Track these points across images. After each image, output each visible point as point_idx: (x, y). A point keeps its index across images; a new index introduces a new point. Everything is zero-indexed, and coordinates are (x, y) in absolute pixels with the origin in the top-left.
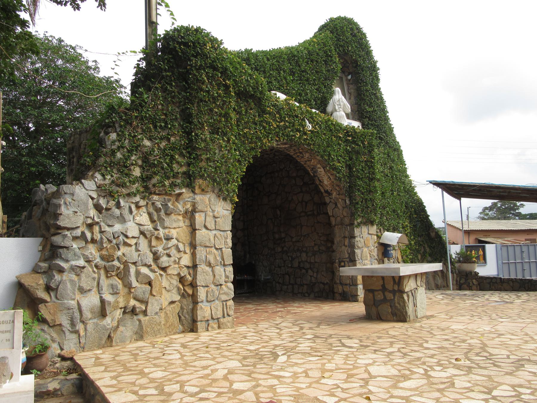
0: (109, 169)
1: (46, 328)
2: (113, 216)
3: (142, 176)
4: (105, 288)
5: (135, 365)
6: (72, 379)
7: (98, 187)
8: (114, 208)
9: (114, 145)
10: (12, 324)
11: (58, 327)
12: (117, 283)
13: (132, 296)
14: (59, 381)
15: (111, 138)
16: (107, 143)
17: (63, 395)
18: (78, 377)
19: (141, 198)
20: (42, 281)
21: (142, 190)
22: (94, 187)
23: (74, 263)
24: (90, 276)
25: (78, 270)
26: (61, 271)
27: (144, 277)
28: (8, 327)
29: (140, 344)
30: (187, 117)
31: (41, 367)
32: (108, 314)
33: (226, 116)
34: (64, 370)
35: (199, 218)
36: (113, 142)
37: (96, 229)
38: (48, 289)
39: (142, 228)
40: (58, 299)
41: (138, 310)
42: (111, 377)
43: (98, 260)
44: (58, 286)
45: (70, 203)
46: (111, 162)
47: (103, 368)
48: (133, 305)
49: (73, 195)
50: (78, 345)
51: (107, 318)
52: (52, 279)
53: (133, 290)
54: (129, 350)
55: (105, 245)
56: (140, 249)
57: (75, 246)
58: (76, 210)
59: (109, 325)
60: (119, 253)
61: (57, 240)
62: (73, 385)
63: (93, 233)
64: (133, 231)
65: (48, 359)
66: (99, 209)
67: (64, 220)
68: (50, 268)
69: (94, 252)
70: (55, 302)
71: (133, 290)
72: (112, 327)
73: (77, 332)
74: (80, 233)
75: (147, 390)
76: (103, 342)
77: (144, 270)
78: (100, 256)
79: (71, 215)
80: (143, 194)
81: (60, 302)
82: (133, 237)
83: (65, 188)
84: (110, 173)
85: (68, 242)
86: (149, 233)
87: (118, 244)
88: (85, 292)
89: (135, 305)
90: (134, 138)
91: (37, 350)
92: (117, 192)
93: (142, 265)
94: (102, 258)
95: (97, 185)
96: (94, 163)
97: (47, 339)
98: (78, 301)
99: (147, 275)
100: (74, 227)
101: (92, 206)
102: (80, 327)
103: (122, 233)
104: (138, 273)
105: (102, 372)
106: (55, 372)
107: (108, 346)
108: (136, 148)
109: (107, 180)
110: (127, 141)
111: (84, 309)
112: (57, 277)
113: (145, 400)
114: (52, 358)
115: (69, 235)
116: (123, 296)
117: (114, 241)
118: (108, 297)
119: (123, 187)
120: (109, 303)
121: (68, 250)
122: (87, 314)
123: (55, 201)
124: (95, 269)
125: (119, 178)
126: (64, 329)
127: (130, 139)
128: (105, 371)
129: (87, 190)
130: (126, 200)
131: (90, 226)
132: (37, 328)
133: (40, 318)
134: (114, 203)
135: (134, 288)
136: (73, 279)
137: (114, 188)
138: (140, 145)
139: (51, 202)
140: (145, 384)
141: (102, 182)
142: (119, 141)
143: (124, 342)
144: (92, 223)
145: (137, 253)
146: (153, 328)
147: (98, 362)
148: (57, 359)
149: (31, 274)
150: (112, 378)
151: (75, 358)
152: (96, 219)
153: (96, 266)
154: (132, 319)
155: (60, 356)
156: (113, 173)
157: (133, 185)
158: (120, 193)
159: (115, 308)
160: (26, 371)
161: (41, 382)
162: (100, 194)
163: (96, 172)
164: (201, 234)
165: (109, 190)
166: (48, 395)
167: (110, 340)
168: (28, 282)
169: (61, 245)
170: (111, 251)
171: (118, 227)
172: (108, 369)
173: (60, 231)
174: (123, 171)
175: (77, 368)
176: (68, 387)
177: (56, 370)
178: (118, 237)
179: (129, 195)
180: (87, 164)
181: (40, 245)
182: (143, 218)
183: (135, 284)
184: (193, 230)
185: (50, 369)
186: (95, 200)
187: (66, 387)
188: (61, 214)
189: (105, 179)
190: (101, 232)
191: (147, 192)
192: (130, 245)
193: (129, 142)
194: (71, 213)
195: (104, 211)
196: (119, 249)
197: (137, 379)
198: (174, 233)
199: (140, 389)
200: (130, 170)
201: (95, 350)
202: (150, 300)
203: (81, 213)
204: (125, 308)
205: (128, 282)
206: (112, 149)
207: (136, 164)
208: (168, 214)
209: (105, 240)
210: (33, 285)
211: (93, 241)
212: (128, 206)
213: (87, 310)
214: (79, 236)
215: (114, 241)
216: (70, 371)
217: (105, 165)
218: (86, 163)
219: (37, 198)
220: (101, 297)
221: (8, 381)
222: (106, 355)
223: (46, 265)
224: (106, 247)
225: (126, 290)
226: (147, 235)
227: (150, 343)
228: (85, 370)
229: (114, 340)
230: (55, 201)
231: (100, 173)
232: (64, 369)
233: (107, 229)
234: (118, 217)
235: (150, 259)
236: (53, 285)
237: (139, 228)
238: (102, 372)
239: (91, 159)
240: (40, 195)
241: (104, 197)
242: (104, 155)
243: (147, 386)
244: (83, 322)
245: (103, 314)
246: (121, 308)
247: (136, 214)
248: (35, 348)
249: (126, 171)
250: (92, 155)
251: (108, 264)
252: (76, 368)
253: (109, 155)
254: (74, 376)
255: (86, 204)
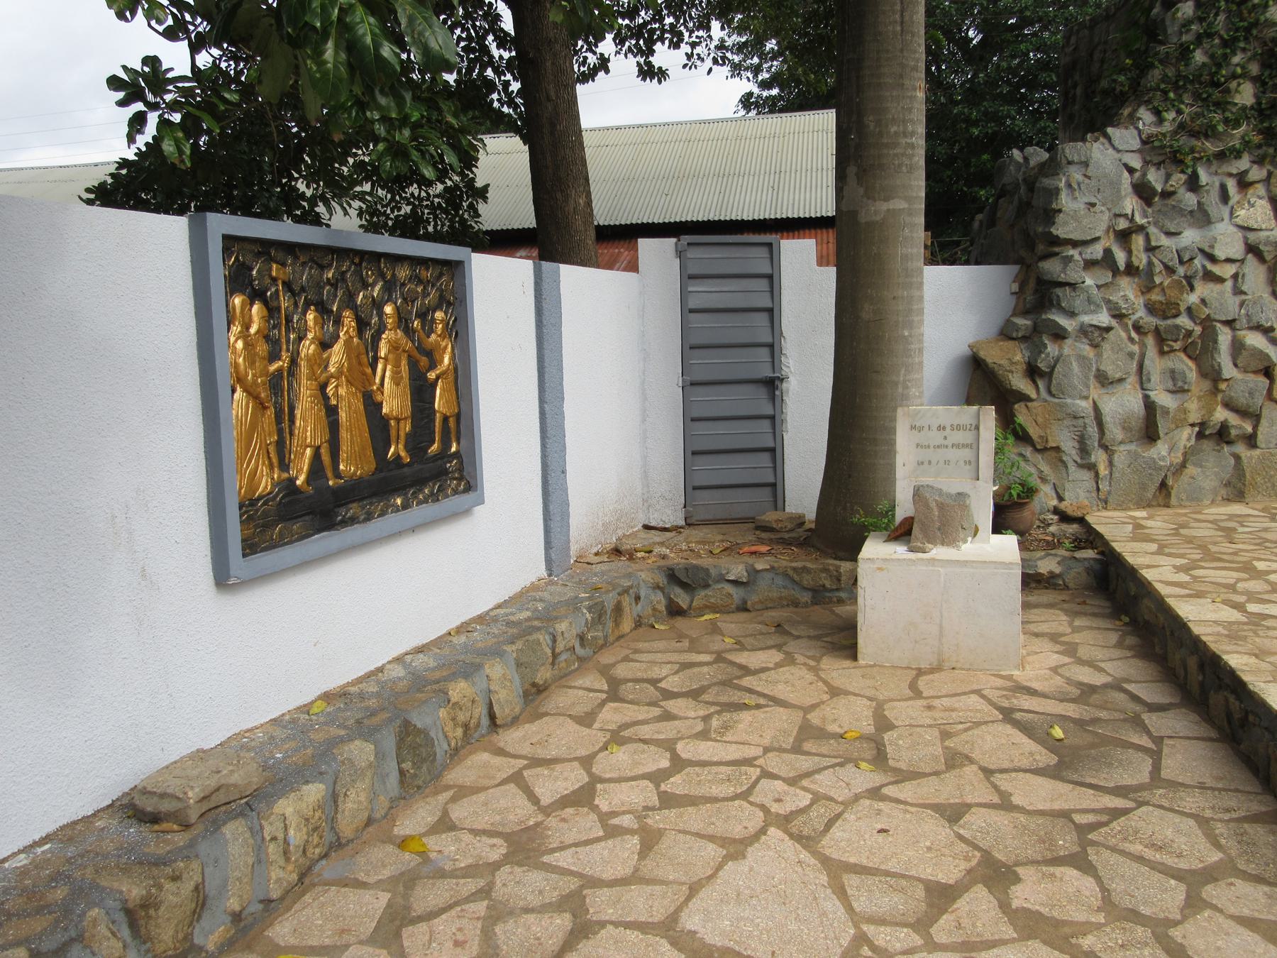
0: (1172, 95)
1: (1028, 451)
2: (1180, 211)
3: (1259, 103)
4: (1155, 378)
5: (1231, 551)
6: (1085, 559)
7: (1144, 142)
8: (1182, 191)
9: (1188, 31)
10: (974, 432)
11: (1053, 454)
12: (1185, 368)
13: (1219, 398)
14: (1059, 559)
15: (1179, 15)
16: (1170, 31)
17: (1067, 587)
18: (1098, 557)
19: (1254, 162)
20: (1019, 355)
21: (1257, 139)
22: (1136, 144)
23: (1086, 319)
24: (1121, 350)
25: (1095, 335)
26: (1059, 335)
27: (1252, 355)
28: (967, 437)
29: (1237, 509)
31: (1022, 527)
32: (1161, 435)
34: (1066, 541)
36: (1184, 26)
37: (1138, 241)
38: (1033, 372)
39: (1252, 237)
40: (1054, 396)
41: (1233, 432)
42: (1175, 567)
43: (1141, 313)
44: (1053, 368)
45: (1079, 184)
46: (1179, 76)
47: (1154, 547)
48: (1222, 419)
49: (1086, 164)
50: (1094, 495)
51: (1159, 443)
52: (1041, 352)
53: (1223, 386)
54: (1211, 518)
55: (1157, 280)
56: (1244, 288)
57: (1089, 282)
58: (1093, 200)
59: (1163, 458)
60: (1193, 298)
61: (1051, 267)
62: (1088, 571)
63: (1130, 252)
64: (1228, 242)
65: (1034, 514)
66: (1145, 195)
67: (1066, 223)
68: (1037, 330)
69: (1131, 296)
70: (1046, 401)
71: (1223, 386)
72: (1171, 465)
73: (1092, 467)
74: (1101, 252)
75: (1267, 606)
76: (1149, 495)
77: (1255, 340)
78: (1145, 306)
79: (1082, 213)
80: (1261, 152)
81: (1056, 400)
82: (1229, 260)
83: (1071, 150)
84: (1174, 106)
85: (1073, 274)
86: (1270, 248)
87: (1191, 277)
88: (1112, 383)
89: (1226, 420)
90: (1243, 7)
91: (1014, 493)
92: (1192, 150)
93: (1251, 328)
94: (1151, 309)
95: (1143, 136)
96: (1135, 85)
97: (1031, 475)
98: (1094, 403)
99: (1261, 351)
100: (1089, 238)
101: (1130, 189)
102: (1099, 457)
103: (1201, 251)
104: (1238, 347)
105: (1152, 554)
106: (1047, 542)
107: (1160, 506)
108: (1248, 30)
109: (1166, 124)
110: (1221, 17)
111: (1107, 419)
112: (1052, 349)
113: (1264, 626)
114: (1040, 514)
115: (1077, 257)
116: (1199, 398)
117: (1181, 271)
118: (1162, 398)
119: (1207, 136)
120: (1166, 412)
121: (1074, 289)
122: (1115, 432)
123: (1047, 182)
124: (1134, 335)
125: (1198, 115)
126: (1064, 459)
127: (1230, 12)
128: (1159, 552)
129: (1119, 151)
130: (1213, 168)
131: (1124, 237)
132: (1012, 449)
133: (1018, 429)
134: (1183, 177)
135: (1226, 380)
136: (1085, 353)
137: (1184, 141)
138: (1256, 24)
139: (1037, 185)
140: (1259, 593)
141: (1154, 130)
142: (1201, 20)
143: (1198, 500)
144: (1129, 228)
145: (1238, 299)
146: (1271, 476)
147: (1140, 532)
148: (1052, 516)
149: (998, 340)
150: (1178, 569)
151: (1089, 518)
152: (1139, 220)
153: (1137, 328)
154: (1219, 451)
155: (1056, 511)
156: (1183, 103)
157: (1233, 129)
158: (1199, 152)
159: (1179, 423)
160: (997, 529)
161: (1027, 555)
162: (1148, 158)
163: (1139, 106)
165: (1171, 146)
166: (1039, 582)
167: (1164, 492)
168: (995, 356)
169: (1060, 280)
170: (1172, 293)
171: (1190, 237)
172: (1167, 550)
173: (1056, 249)
174: (1210, 96)
175: (1094, 539)
176: (1079, 573)
177: (1049, 538)
178: (1191, 259)
179: (1221, 156)
180: (1118, 89)
181: (1014, 282)
183: (1228, 370)
185: (1037, 534)
186: (1137, 175)
187: (1073, 573)
188: (1060, 211)
189: (1161, 121)
190: (1150, 249)
191: (1270, 145)
192: (1220, 280)
193: (1226, 18)
194: (1082, 206)
195: (1156, 199)
196: (1192, 288)
197: (1238, 580)
199: (1248, 601)
200: (1228, 91)
201: (1130, 509)
202: (1265, 412)
203: (1103, 205)
204: (1202, 425)
205: (1212, 366)
206: (1182, 45)
207: (1244, 75)
209: (1159, 267)
210: (1002, 362)
211: (1131, 270)
212: (1217, 184)
213: (1114, 423)
214: (1099, 258)
215: (1181, 271)
216: (1079, 544)
217: (1163, 86)
218: (1114, 89)
219: (1006, 179)
220: (1146, 397)
221: (970, 539)
222: (1158, 522)
223: (1028, 323)
224: (1161, 283)
225: (1206, 385)
226: (1266, 254)
227: (1263, 510)
228: (1114, 545)
229: (1173, 493)
230: (1047, 182)
231: (1150, 107)
232: (1067, 538)
233: (1165, 241)
234: (1191, 212)
236: (1042, 365)
237: (1246, 239)
238: (1152, 554)
239: (1129, 75)
240: (1013, 172)
241: (1158, 165)
242: (1161, 62)
243: (1266, 597)
244: (1105, 448)
245: (1150, 433)
246: (1193, 425)
247: (1238, 202)
248: (1010, 488)
249: (1216, 95)
250: (1132, 65)
251: (1163, 324)
252: (1091, 538)
253: (1174, 61)
254: (1089, 554)
255: (1115, 185)
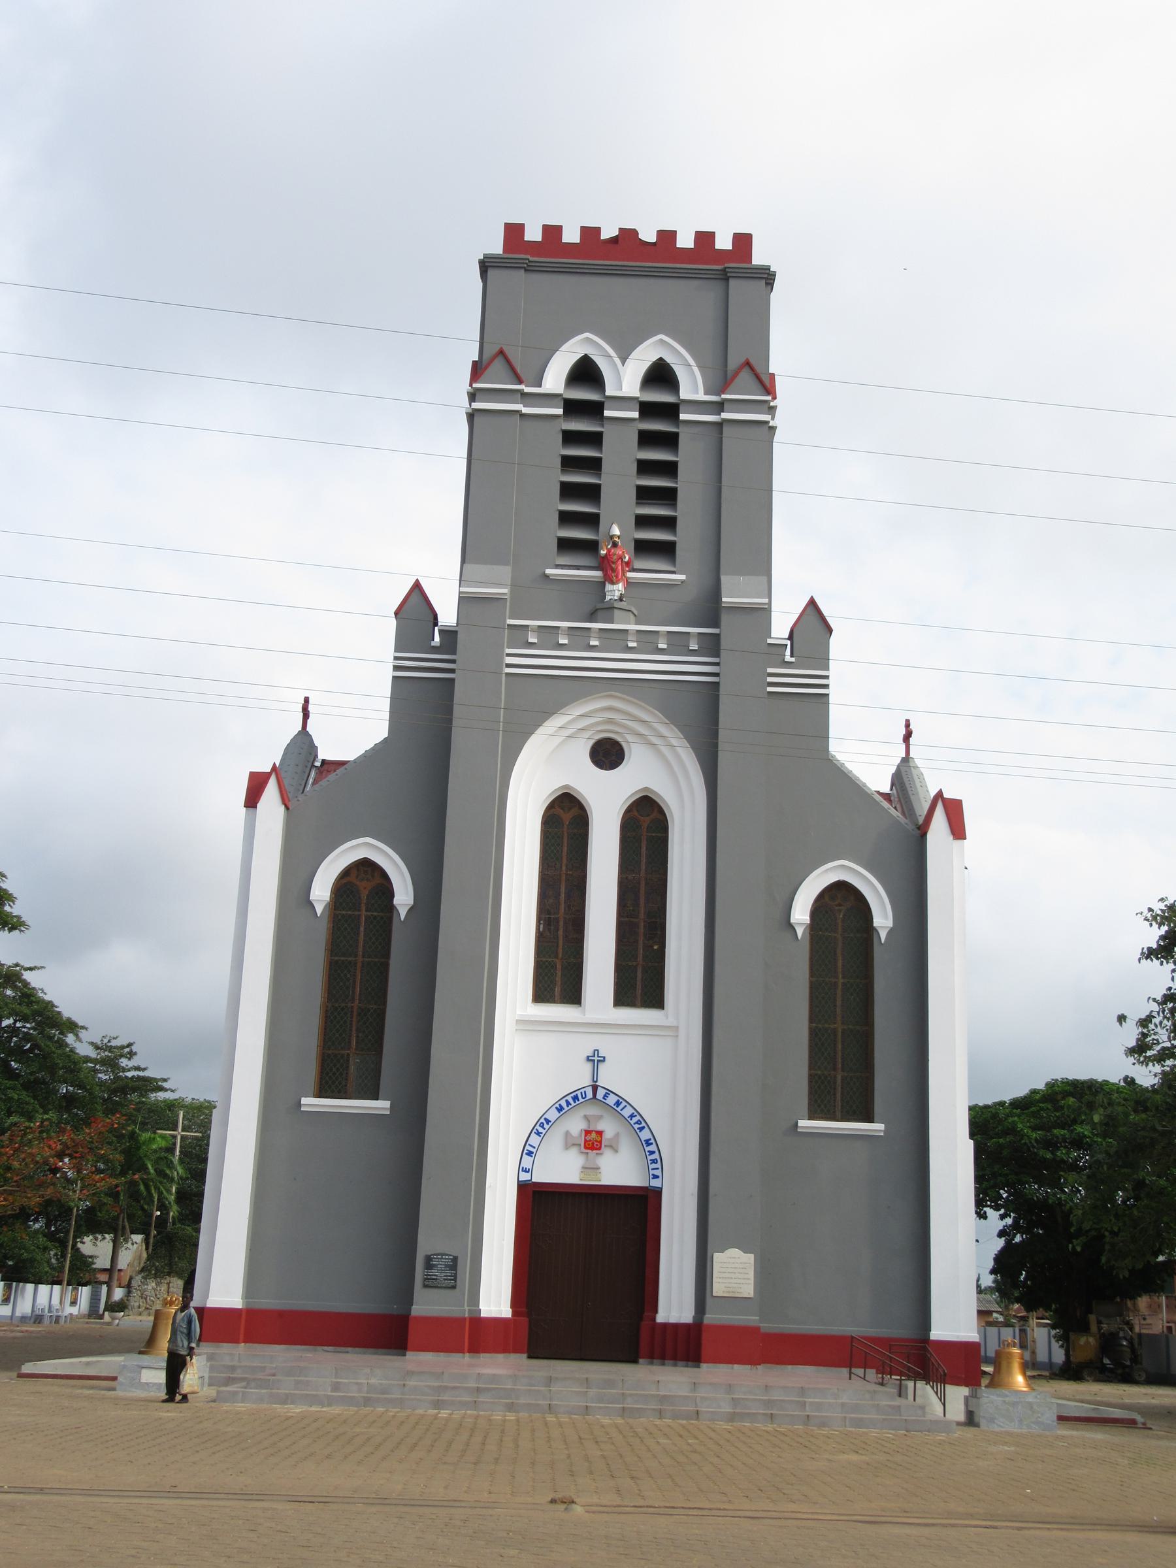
20: (126, 1298)
25: (134, 1297)
30: (171, 1256)
33: (184, 1254)
35: (171, 1285)
77: (152, 1298)
131: (139, 1286)
164: (171, 1289)
171: (146, 1287)
182: (154, 1284)
184: (169, 1288)
198: (163, 1289)
208: (161, 1283)
235: (154, 1295)
245: (139, 1308)
